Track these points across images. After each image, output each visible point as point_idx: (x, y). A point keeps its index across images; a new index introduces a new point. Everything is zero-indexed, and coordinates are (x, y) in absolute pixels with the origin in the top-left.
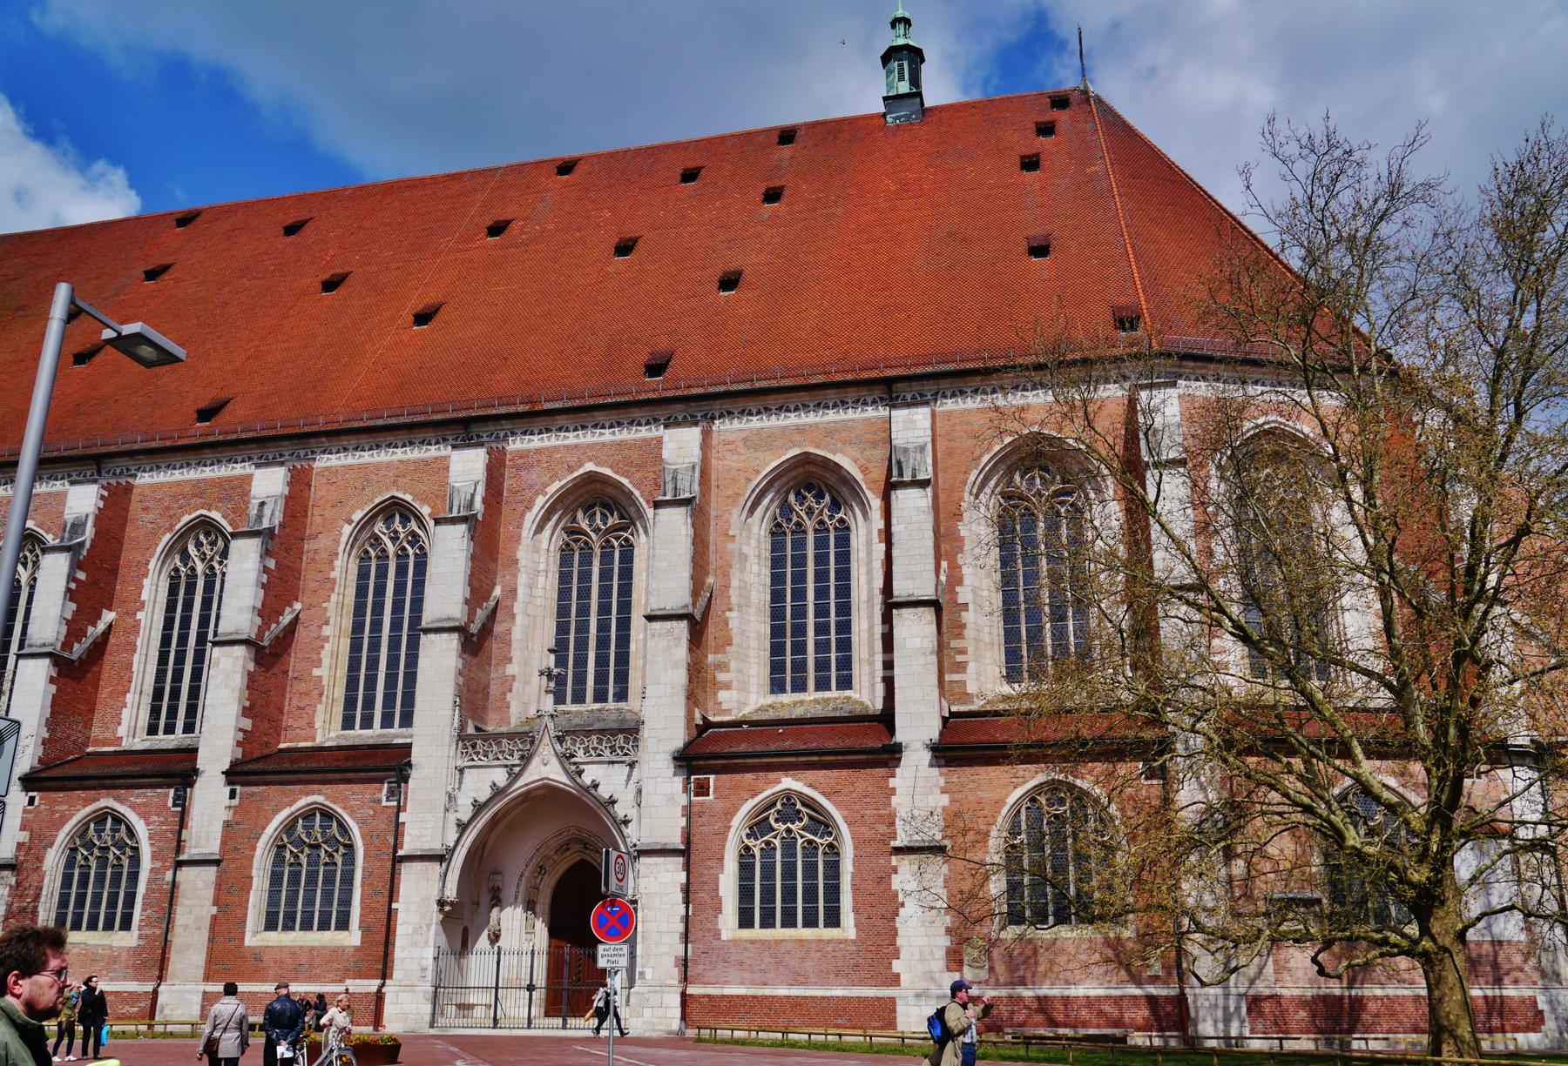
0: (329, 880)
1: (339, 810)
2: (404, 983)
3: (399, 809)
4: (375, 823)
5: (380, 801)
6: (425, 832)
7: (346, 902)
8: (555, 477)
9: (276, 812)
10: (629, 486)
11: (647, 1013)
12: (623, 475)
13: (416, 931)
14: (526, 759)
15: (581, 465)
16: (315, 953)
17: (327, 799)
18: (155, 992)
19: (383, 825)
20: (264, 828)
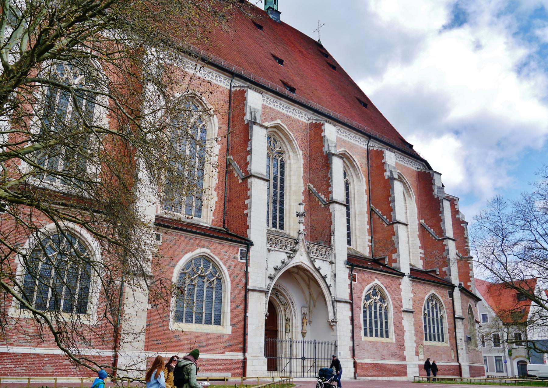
0: (209, 297)
1: (218, 260)
2: (253, 355)
3: (247, 265)
4: (235, 270)
5: (237, 258)
7: (219, 310)
9: (184, 253)
14: (295, 251)
15: (276, 119)
16: (209, 337)
17: (211, 251)
18: (116, 357)
19: (239, 271)
20: (178, 262)
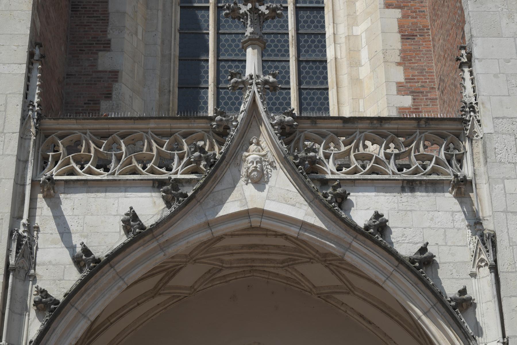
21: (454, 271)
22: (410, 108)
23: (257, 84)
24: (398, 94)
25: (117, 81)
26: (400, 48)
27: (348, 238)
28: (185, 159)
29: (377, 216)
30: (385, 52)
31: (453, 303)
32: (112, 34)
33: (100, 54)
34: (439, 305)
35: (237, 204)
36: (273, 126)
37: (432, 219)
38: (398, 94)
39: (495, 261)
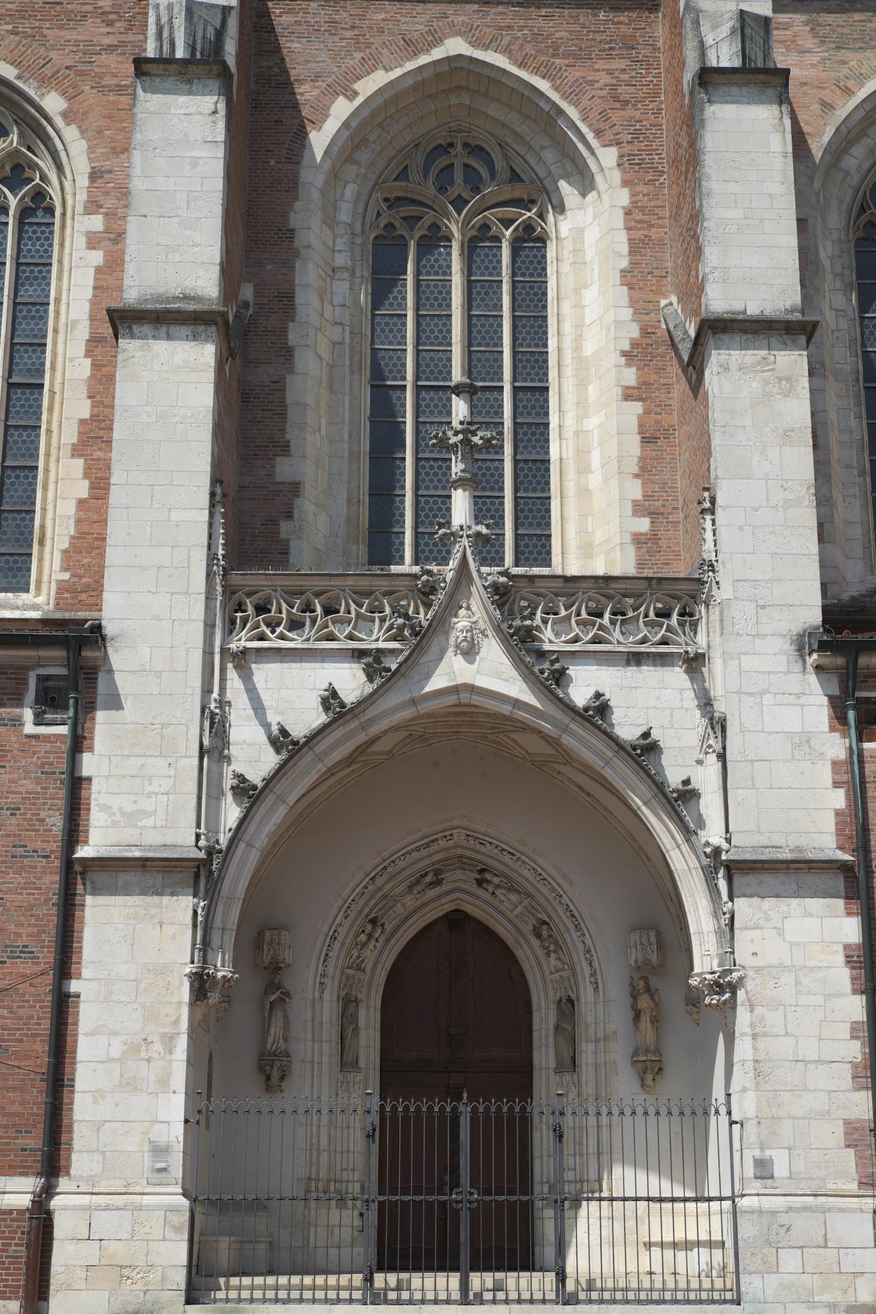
6: (147, 804)
8: (369, 66)
10: (554, 96)
11: (790, 1260)
12: (536, 71)
13: (133, 1050)
15: (438, 41)
21: (679, 757)
22: (645, 534)
23: (468, 536)
24: (633, 515)
25: (298, 496)
26: (639, 454)
27: (566, 720)
28: (387, 624)
29: (598, 695)
30: (620, 460)
31: (675, 795)
32: (291, 434)
33: (278, 459)
34: (660, 796)
35: (445, 678)
36: (485, 588)
37: (658, 698)
38: (633, 515)
39: (724, 748)
